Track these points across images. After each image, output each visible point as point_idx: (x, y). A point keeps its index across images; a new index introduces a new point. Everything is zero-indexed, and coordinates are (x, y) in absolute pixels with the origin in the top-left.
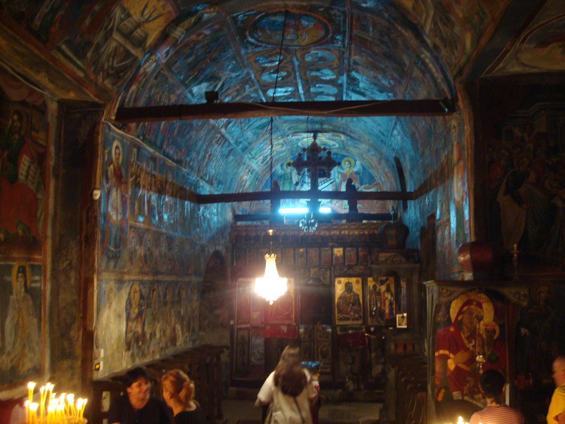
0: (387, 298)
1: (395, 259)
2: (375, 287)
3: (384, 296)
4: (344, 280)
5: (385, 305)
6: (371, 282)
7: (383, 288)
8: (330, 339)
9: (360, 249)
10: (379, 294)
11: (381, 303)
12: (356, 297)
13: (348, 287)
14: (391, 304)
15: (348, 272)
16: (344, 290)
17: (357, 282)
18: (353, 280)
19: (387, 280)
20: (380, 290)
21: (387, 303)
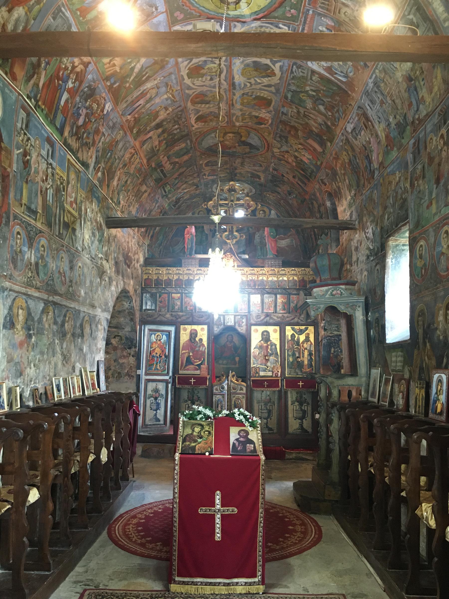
0: (306, 349)
1: (334, 293)
2: (293, 336)
3: (303, 346)
4: (262, 329)
5: (303, 357)
6: (289, 331)
7: (302, 338)
8: (244, 391)
9: (278, 296)
10: (298, 343)
11: (299, 354)
12: (273, 347)
13: (266, 337)
14: (310, 354)
15: (265, 320)
16: (261, 339)
17: (275, 331)
18: (270, 329)
19: (306, 329)
20: (298, 339)
21: (306, 353)
